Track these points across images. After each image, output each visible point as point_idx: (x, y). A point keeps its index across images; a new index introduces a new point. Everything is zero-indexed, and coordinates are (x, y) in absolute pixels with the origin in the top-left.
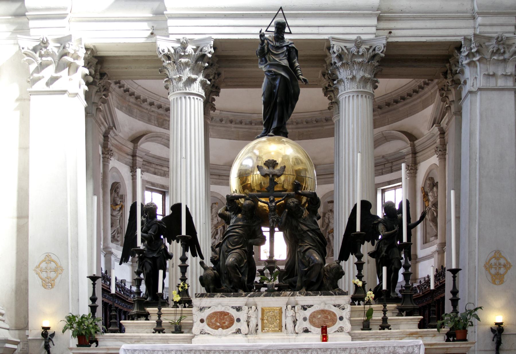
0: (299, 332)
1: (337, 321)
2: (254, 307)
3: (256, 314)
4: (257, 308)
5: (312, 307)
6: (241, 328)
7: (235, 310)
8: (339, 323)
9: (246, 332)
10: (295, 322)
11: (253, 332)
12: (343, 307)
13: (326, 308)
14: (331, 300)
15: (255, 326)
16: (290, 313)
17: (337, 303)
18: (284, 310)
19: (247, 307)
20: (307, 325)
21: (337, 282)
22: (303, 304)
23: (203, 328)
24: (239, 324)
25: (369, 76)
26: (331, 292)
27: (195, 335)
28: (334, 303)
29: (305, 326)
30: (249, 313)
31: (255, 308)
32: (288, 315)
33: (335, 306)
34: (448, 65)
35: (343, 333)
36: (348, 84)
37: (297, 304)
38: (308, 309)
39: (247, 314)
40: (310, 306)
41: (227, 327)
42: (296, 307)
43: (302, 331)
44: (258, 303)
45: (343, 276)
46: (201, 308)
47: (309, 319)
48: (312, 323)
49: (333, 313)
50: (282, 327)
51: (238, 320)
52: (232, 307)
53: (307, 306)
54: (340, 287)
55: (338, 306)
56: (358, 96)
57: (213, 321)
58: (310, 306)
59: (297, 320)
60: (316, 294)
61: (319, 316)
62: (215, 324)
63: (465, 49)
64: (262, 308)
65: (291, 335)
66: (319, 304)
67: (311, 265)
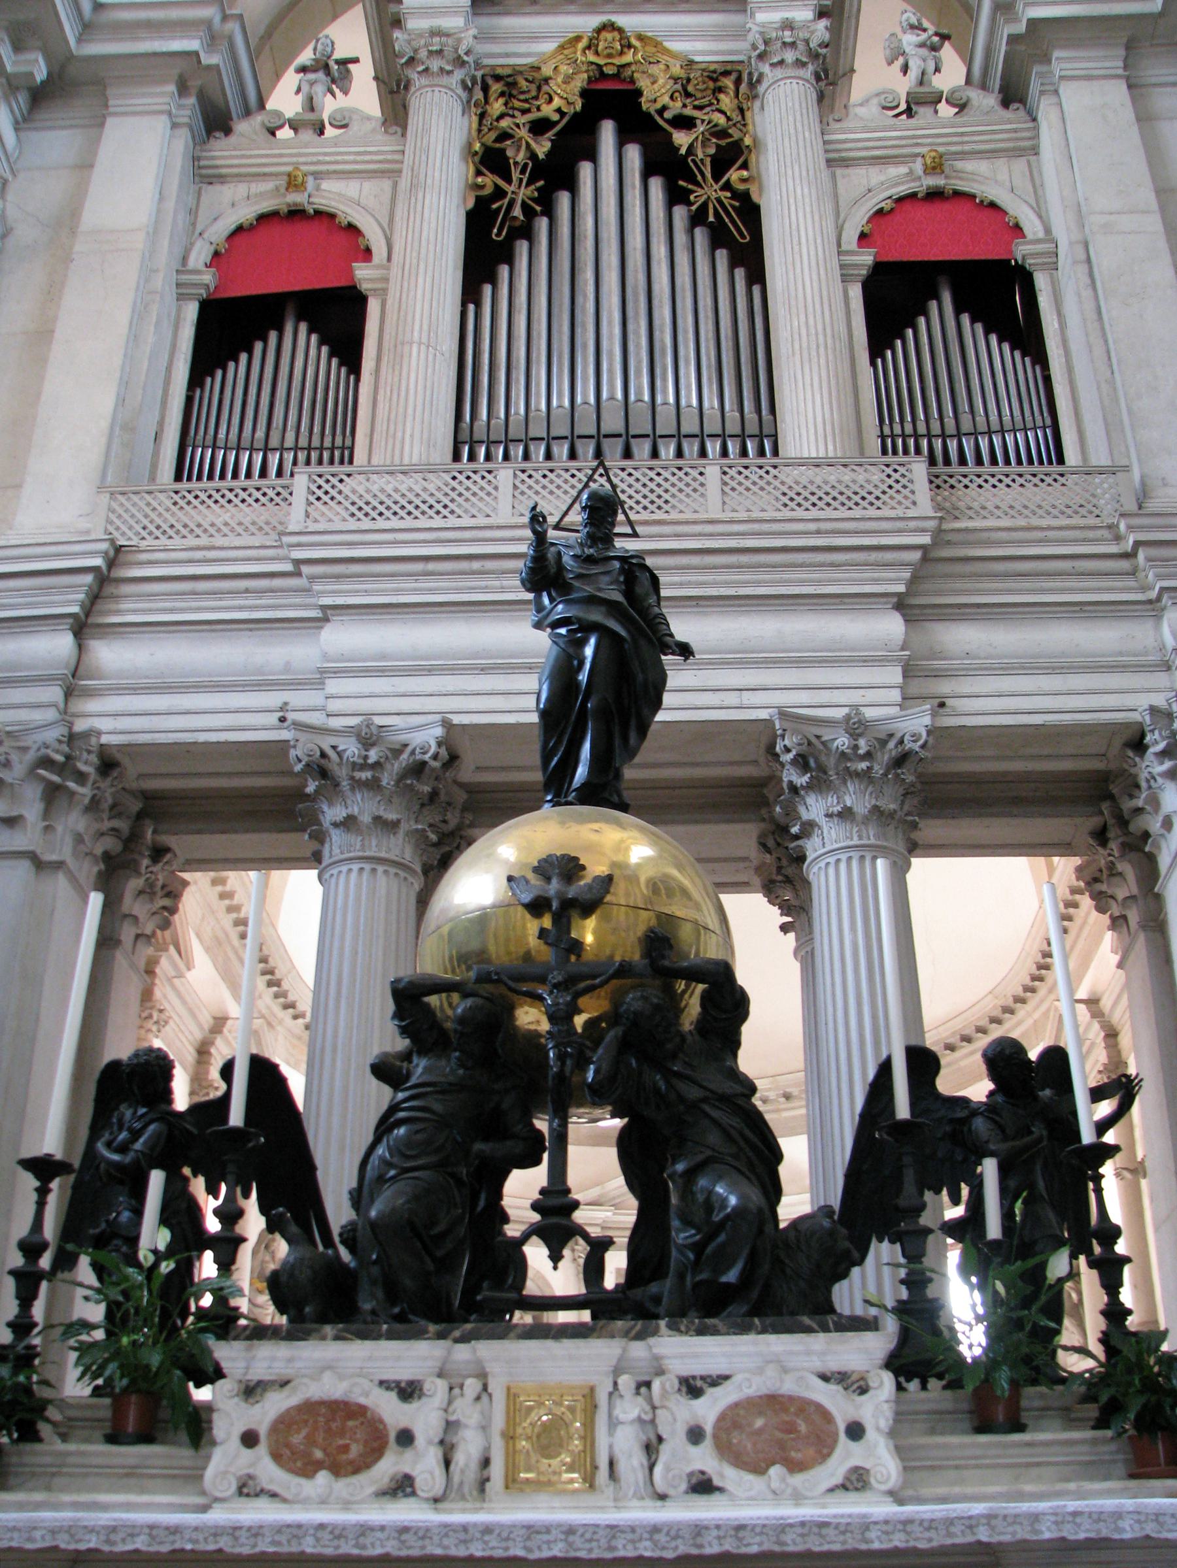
0: (671, 1492)
1: (836, 1441)
2: (472, 1386)
3: (482, 1413)
4: (485, 1388)
5: (728, 1382)
6: (414, 1474)
7: (393, 1396)
8: (848, 1455)
9: (438, 1490)
10: (651, 1448)
11: (466, 1489)
12: (862, 1383)
13: (789, 1387)
14: (808, 1353)
15: (474, 1465)
16: (630, 1408)
17: (833, 1364)
18: (602, 1398)
19: (441, 1385)
20: (704, 1459)
21: (829, 1292)
22: (685, 1373)
23: (251, 1471)
24: (409, 1454)
25: (892, 806)
26: (806, 1320)
27: (217, 1500)
28: (818, 1365)
29: (698, 1466)
30: (451, 1409)
31: (479, 1387)
32: (622, 1417)
33: (825, 1378)
34: (1105, 807)
35: (867, 1495)
36: (833, 831)
37: (660, 1372)
38: (711, 1392)
39: (446, 1411)
40: (717, 1381)
41: (358, 1467)
42: (656, 1385)
43: (684, 1486)
44: (493, 1368)
45: (856, 1271)
46: (252, 1384)
47: (715, 1437)
48: (728, 1451)
49: (819, 1408)
50: (596, 1468)
51: (406, 1438)
52: (381, 1383)
53: (703, 1378)
54: (839, 1311)
55: (840, 1378)
56: (862, 858)
57: (297, 1439)
58: (717, 1381)
59: (660, 1439)
60: (743, 1329)
61: (759, 1423)
62: (307, 1455)
63: (1157, 735)
64: (509, 1389)
65: (635, 1503)
66: (760, 1371)
67: (717, 1217)
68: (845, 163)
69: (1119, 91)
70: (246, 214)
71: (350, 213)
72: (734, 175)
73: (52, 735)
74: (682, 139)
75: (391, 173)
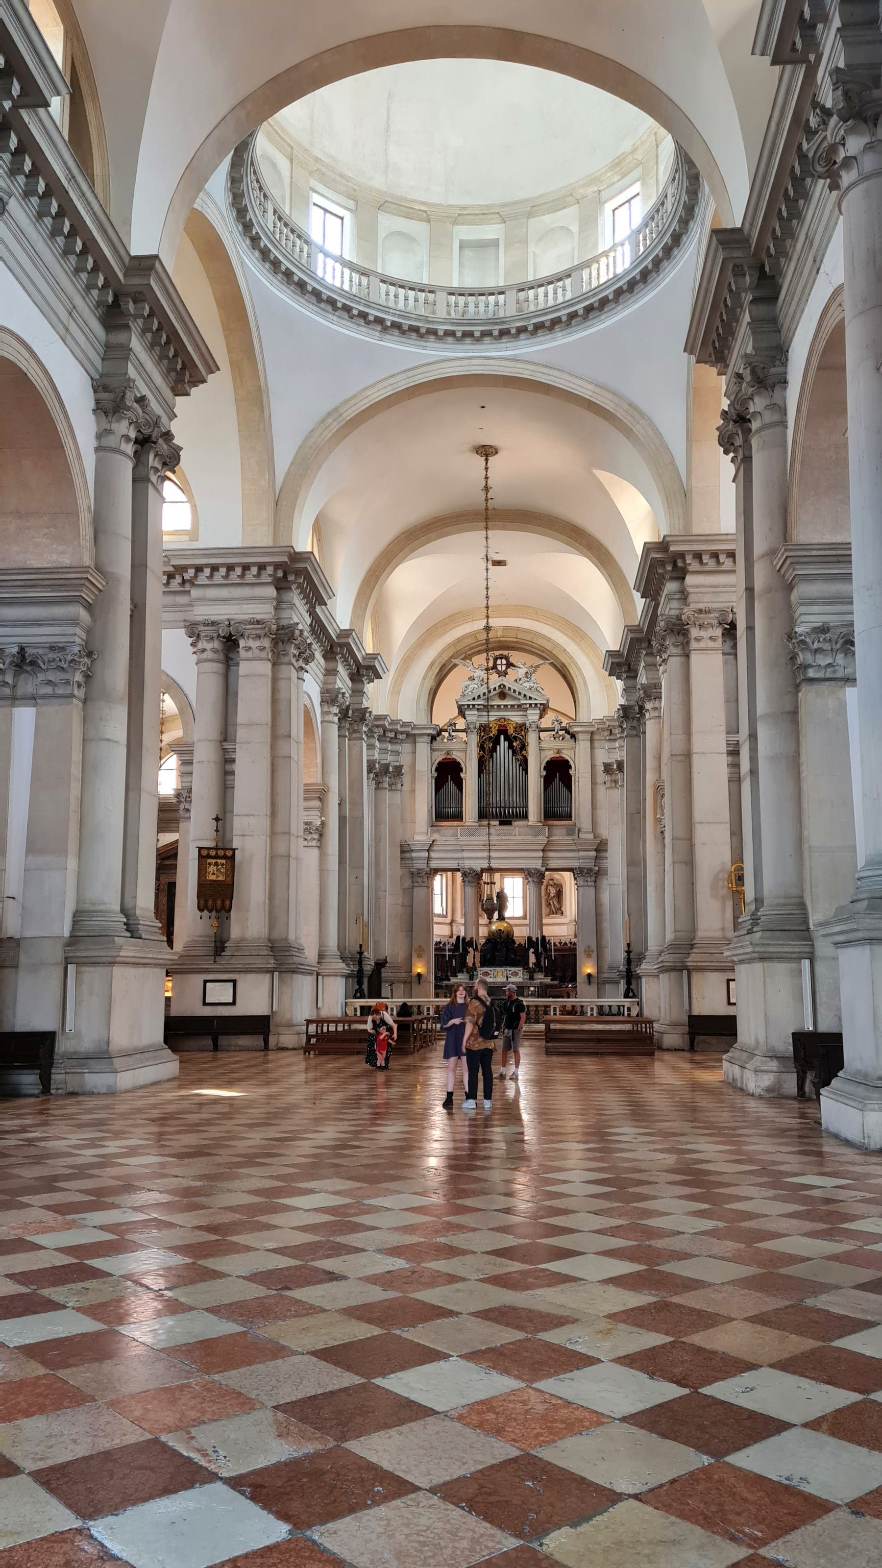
68: (543, 750)
69: (589, 743)
70: (440, 759)
71: (459, 760)
72: (524, 752)
73: (428, 869)
74: (515, 744)
75: (465, 751)
